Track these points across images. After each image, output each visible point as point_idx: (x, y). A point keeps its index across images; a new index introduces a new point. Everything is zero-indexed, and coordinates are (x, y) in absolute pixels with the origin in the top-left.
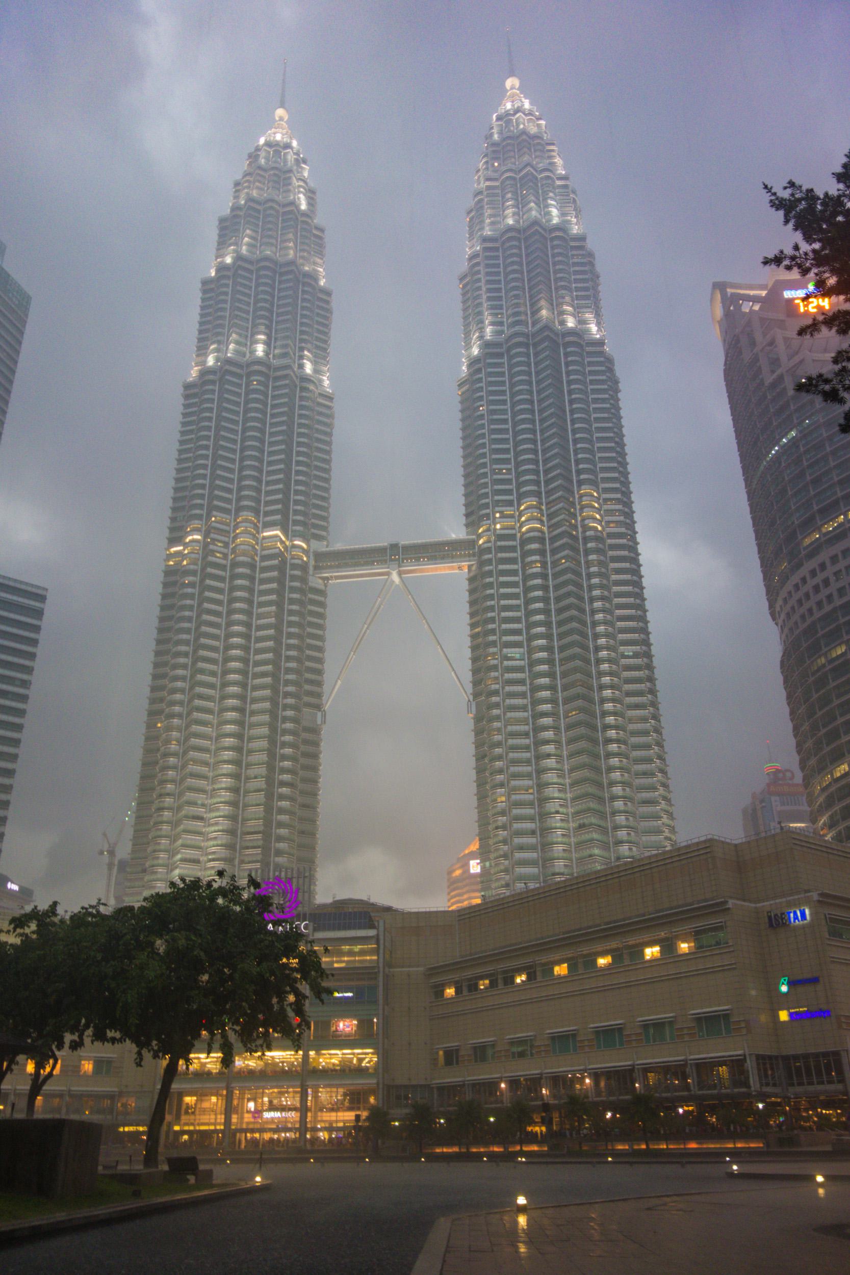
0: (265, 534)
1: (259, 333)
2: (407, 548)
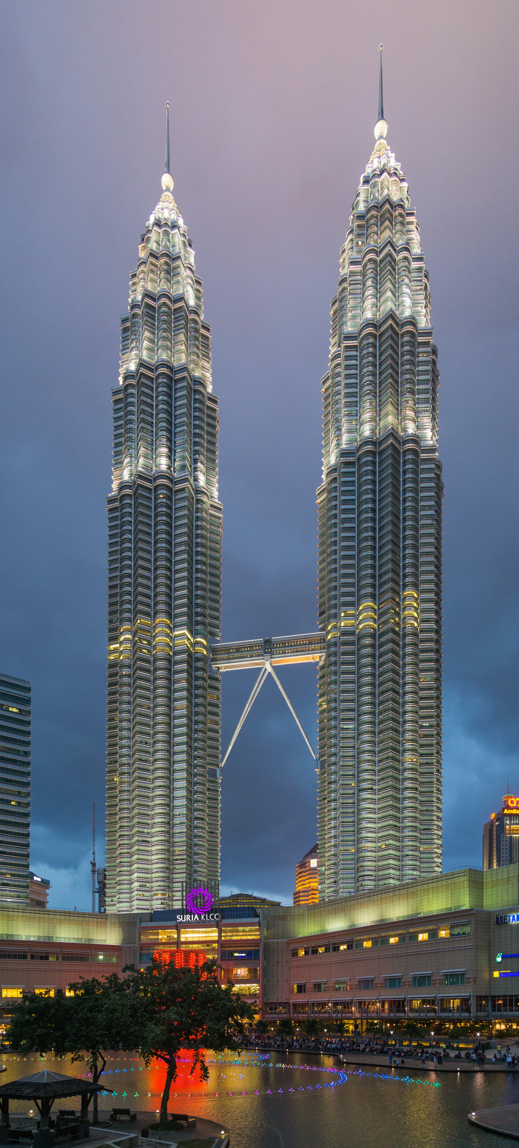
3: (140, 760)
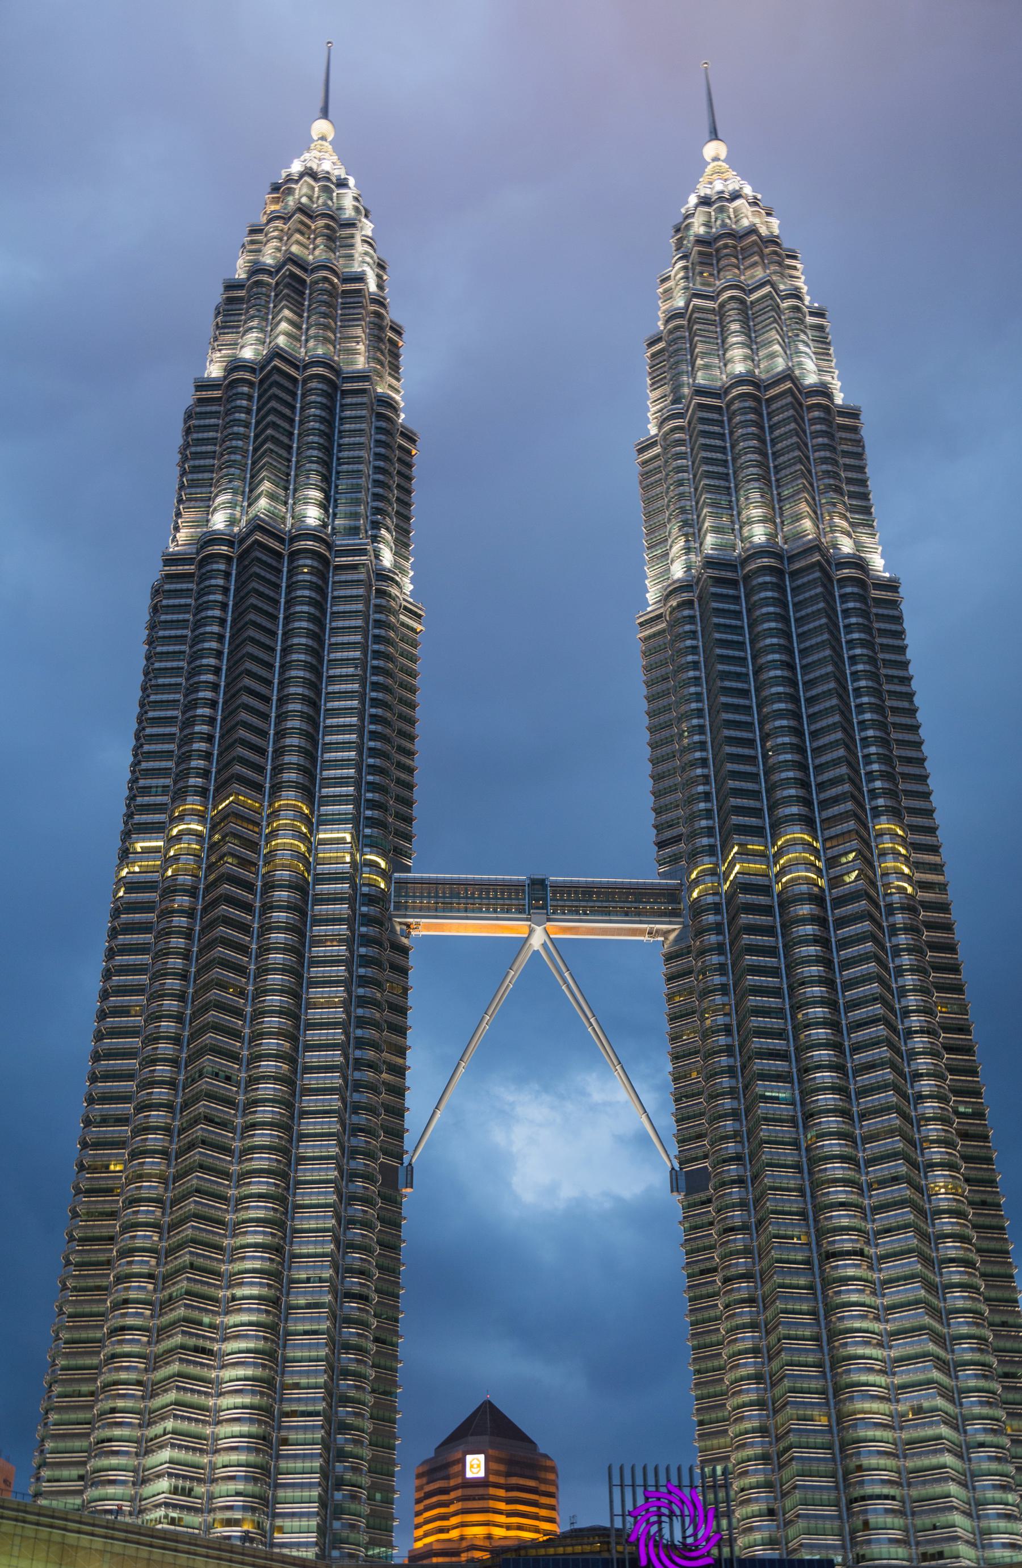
0: (321, 836)
1: (307, 486)
2: (560, 889)
3: (210, 1120)
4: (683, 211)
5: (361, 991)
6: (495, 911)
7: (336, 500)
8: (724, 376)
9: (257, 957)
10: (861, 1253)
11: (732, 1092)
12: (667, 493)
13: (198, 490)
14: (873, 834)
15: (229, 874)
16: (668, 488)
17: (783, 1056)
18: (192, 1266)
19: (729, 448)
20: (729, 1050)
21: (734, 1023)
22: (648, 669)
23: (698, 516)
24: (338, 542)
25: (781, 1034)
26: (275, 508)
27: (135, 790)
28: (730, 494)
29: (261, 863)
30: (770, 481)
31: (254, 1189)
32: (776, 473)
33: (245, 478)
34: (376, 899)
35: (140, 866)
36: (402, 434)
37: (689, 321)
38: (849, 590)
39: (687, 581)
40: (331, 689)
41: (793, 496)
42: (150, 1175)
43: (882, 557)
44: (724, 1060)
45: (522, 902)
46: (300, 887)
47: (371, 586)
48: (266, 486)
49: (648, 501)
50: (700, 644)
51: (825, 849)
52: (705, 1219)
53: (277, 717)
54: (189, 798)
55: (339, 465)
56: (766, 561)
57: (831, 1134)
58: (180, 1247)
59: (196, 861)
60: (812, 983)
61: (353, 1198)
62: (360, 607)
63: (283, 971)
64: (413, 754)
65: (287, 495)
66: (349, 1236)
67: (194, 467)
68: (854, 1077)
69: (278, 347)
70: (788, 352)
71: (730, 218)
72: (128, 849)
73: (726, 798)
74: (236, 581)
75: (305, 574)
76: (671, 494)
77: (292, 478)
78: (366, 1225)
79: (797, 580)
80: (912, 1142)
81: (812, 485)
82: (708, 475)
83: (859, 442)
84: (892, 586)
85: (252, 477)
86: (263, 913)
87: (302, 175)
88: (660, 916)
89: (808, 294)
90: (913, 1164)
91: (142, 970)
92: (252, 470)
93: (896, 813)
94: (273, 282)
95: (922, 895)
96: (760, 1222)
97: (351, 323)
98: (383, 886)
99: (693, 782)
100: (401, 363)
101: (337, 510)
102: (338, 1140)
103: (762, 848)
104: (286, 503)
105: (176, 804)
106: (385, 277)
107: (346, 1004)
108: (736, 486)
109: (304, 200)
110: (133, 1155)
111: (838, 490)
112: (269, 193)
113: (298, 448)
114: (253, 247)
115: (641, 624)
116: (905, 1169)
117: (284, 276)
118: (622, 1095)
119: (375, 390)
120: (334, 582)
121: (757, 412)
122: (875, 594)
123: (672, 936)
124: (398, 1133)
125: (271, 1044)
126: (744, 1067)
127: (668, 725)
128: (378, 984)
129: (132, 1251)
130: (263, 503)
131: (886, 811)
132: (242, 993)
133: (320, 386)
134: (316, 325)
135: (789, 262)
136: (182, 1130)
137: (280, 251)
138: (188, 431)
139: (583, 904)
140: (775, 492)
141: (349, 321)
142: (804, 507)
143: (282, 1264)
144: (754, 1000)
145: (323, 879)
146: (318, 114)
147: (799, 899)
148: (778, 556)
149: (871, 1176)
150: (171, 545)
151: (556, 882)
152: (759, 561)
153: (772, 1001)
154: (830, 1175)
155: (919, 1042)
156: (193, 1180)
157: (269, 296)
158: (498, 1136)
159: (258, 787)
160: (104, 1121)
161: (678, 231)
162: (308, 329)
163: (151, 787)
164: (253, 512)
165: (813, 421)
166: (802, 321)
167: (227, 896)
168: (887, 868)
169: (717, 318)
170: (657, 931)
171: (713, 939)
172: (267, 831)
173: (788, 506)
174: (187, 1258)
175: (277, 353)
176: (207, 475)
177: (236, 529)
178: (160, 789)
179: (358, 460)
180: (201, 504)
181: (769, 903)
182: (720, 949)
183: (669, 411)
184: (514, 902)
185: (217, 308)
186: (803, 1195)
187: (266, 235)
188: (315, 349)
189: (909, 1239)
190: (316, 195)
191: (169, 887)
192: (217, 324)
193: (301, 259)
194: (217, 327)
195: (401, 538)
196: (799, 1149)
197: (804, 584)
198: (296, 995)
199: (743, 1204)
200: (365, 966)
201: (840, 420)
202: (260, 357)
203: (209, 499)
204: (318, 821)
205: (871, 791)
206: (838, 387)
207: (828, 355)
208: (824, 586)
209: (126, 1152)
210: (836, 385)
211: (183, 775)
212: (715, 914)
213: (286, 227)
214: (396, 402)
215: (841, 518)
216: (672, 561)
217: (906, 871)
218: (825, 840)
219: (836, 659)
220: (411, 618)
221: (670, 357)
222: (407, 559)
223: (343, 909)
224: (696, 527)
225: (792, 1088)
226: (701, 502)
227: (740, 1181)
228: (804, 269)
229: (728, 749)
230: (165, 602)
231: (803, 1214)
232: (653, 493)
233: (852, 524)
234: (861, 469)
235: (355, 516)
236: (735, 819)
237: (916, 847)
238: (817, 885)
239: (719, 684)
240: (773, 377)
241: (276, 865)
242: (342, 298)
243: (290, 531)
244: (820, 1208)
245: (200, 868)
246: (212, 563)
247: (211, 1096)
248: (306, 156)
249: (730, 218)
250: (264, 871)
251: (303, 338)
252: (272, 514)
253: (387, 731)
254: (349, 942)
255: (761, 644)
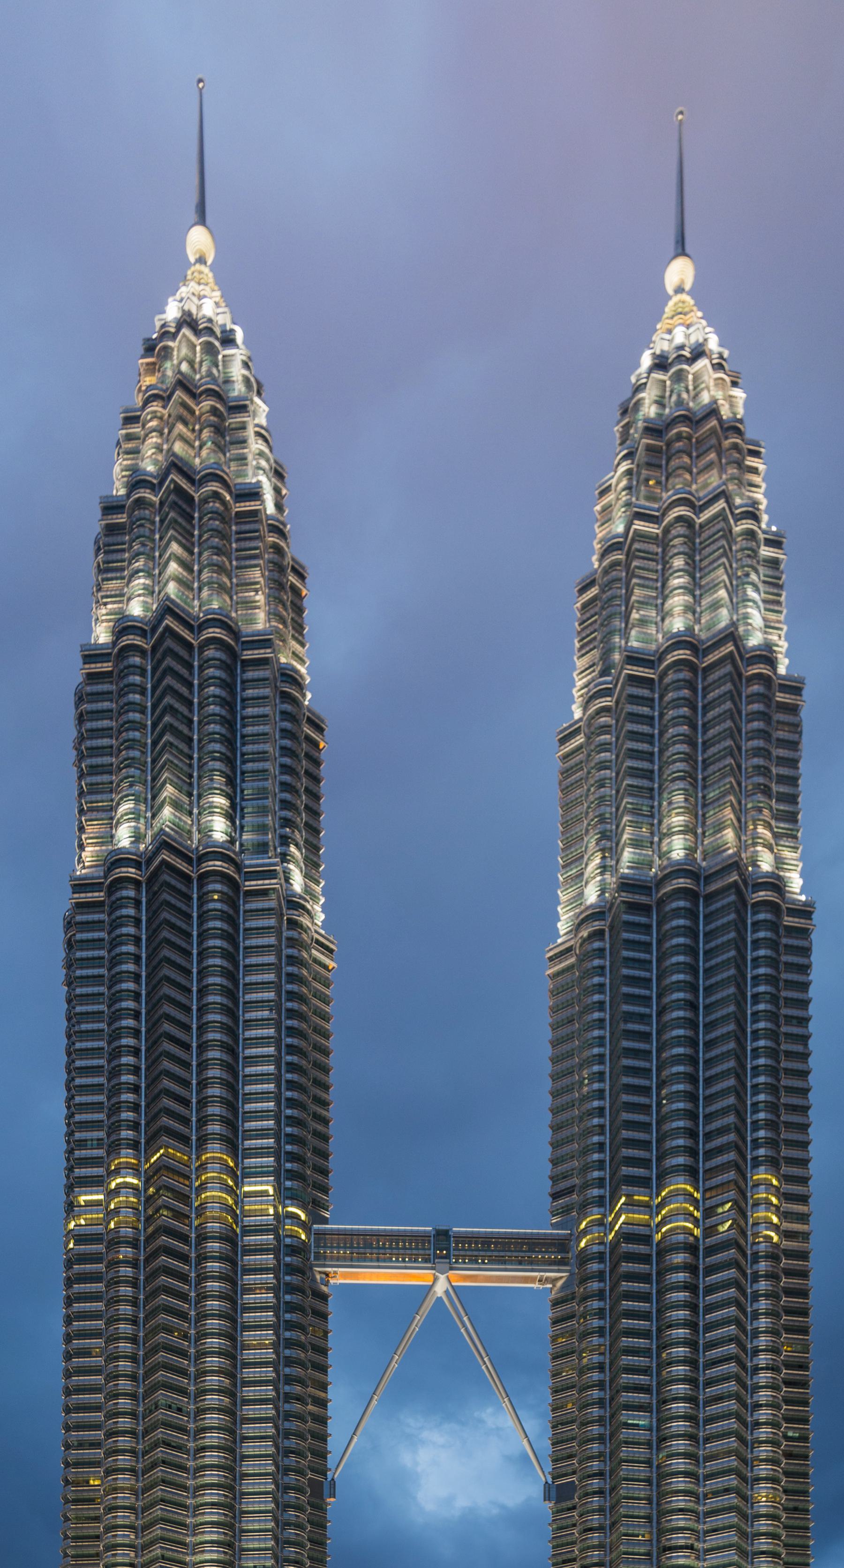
0: (247, 1189)
3: (167, 1444)
4: (633, 379)
5: (288, 1334)
6: (404, 1261)
7: (242, 809)
8: (660, 636)
9: (196, 1304)
10: (691, 1547)
11: (601, 1421)
12: (587, 796)
13: (99, 797)
14: (750, 1184)
15: (165, 1227)
16: (589, 790)
17: (646, 1389)
18: (163, 1557)
19: (657, 737)
20: (601, 1385)
21: (607, 1361)
22: (554, 1010)
23: (617, 826)
24: (247, 862)
25: (646, 1371)
26: (180, 819)
27: (73, 1145)
28: (652, 798)
29: (193, 1216)
30: (696, 780)
31: (208, 1499)
32: (704, 769)
33: (146, 781)
34: (299, 1249)
35: (85, 1219)
36: (310, 721)
37: (627, 555)
38: (762, 916)
39: (600, 907)
40: (248, 1034)
41: (718, 799)
42: (123, 1488)
43: (801, 876)
44: (595, 1393)
45: (427, 1252)
46: (230, 1238)
47: (282, 915)
48: (169, 791)
49: (567, 807)
50: (608, 981)
51: (704, 1199)
52: (569, 1522)
53: (199, 1065)
54: (123, 1152)
55: (244, 762)
56: (682, 882)
57: (679, 1454)
58: (152, 1543)
59: (134, 1214)
60: (678, 1326)
61: (287, 1506)
62: (272, 940)
63: (220, 1316)
64: (328, 1104)
65: (191, 803)
66: (286, 1535)
67: (92, 767)
68: (704, 1407)
69: (168, 598)
70: (735, 600)
71: (688, 391)
72: (72, 1202)
73: (618, 1132)
74: (147, 910)
75: (215, 903)
76: (591, 798)
77: (195, 780)
78: (299, 1526)
79: (711, 904)
80: (744, 1461)
81: (739, 784)
82: (633, 772)
83: (796, 727)
84: (805, 912)
85: (154, 779)
86: (198, 1263)
87: (180, 323)
88: (550, 1264)
89: (766, 512)
90: (743, 1478)
91: (97, 1316)
92: (152, 770)
93: (773, 1163)
94: (156, 500)
95: (787, 1244)
96: (613, 1524)
97: (248, 563)
98: (303, 1237)
99: (588, 1132)
100: (306, 621)
101: (244, 822)
102: (274, 1460)
103: (647, 1199)
104: (190, 813)
105: (111, 1158)
106: (284, 492)
107: (275, 1345)
108: (660, 787)
109: (184, 367)
110: (108, 1473)
111: (766, 791)
112: (143, 357)
113: (200, 741)
114: (130, 445)
115: (551, 959)
116: (736, 1482)
117: (168, 492)
118: (508, 1421)
119: (278, 660)
120: (245, 911)
121: (691, 685)
122: (789, 921)
123: (559, 1284)
124: (322, 1455)
125: (213, 1380)
126: (612, 1399)
127: (570, 1072)
128: (302, 1328)
129: (115, 1546)
130: (167, 812)
131: (766, 1161)
132: (185, 1337)
133: (218, 654)
134: (209, 565)
135: (751, 461)
136: (145, 1453)
137: (161, 451)
138: (81, 719)
139: (482, 1253)
140: (700, 795)
141: (246, 559)
142: (728, 814)
143: (234, 1556)
144: (626, 1341)
145: (250, 1231)
146: (193, 216)
147: (675, 1248)
148: (694, 875)
149: (708, 1488)
150: (78, 868)
151: (459, 1232)
152: (675, 881)
153: (642, 1342)
154: (674, 1487)
155: (764, 1377)
156: (158, 1492)
157: (153, 523)
158: (406, 1459)
159: (185, 1140)
160: (81, 1445)
161: (625, 412)
162: (200, 572)
163: (86, 1140)
164: (157, 824)
165: (753, 698)
166: (755, 552)
167: (165, 1247)
168: (758, 1218)
169: (660, 550)
170: (547, 1279)
171: (595, 1285)
172: (197, 1184)
173: (711, 813)
174: (159, 1551)
175: (168, 609)
176: (105, 778)
177: (142, 847)
178: (95, 1142)
179: (262, 756)
180: (104, 815)
181: (648, 1252)
182: (600, 1295)
183: (596, 686)
184: (421, 1252)
185: (96, 542)
186: (650, 1503)
187: (144, 426)
188: (210, 602)
189: (732, 1537)
190: (198, 360)
191: (113, 1239)
192: (99, 566)
193: (186, 463)
194: (100, 571)
195: (311, 856)
196: (651, 1467)
197: (717, 910)
198: (232, 1338)
199: (601, 1510)
200: (290, 1312)
201: (780, 697)
202: (149, 614)
203: (111, 809)
204: (242, 1173)
205: (755, 1141)
206: (783, 650)
207: (779, 603)
208: (738, 912)
209: (101, 1470)
210: (782, 646)
211: (114, 1128)
212: (599, 1263)
213: (166, 412)
214: (301, 676)
215: (765, 828)
216: (587, 883)
217: (775, 1220)
218: (705, 1191)
219: (739, 998)
220: (323, 953)
221: (603, 608)
222: (317, 883)
223: (269, 1259)
224: (614, 840)
225: (651, 1417)
226: (622, 808)
227: (600, 1492)
228: (767, 472)
229: (625, 1098)
230: (79, 936)
231: (648, 1518)
232: (572, 797)
233: (776, 836)
234: (793, 763)
235: (262, 829)
236: (625, 1170)
237: (788, 1197)
238: (692, 1235)
239: (622, 1026)
240: (714, 636)
241: (207, 1218)
242: (237, 524)
243: (197, 848)
244: (662, 1513)
245: (139, 1220)
246: (121, 888)
247: (167, 1425)
248: (183, 291)
249: (688, 391)
250: (196, 1223)
251: (196, 585)
252: (177, 827)
253: (303, 1080)
254: (276, 1290)
255: (668, 981)
